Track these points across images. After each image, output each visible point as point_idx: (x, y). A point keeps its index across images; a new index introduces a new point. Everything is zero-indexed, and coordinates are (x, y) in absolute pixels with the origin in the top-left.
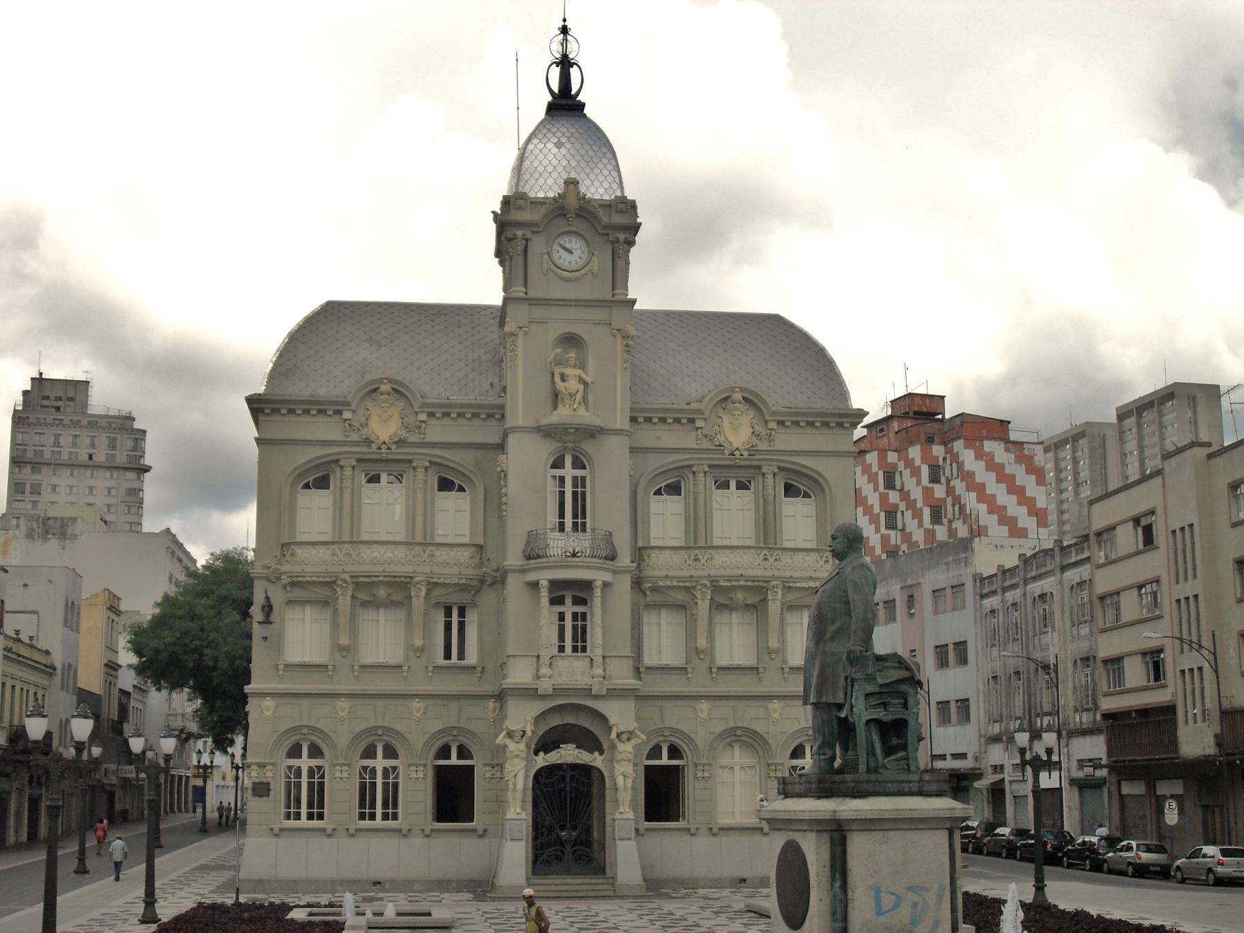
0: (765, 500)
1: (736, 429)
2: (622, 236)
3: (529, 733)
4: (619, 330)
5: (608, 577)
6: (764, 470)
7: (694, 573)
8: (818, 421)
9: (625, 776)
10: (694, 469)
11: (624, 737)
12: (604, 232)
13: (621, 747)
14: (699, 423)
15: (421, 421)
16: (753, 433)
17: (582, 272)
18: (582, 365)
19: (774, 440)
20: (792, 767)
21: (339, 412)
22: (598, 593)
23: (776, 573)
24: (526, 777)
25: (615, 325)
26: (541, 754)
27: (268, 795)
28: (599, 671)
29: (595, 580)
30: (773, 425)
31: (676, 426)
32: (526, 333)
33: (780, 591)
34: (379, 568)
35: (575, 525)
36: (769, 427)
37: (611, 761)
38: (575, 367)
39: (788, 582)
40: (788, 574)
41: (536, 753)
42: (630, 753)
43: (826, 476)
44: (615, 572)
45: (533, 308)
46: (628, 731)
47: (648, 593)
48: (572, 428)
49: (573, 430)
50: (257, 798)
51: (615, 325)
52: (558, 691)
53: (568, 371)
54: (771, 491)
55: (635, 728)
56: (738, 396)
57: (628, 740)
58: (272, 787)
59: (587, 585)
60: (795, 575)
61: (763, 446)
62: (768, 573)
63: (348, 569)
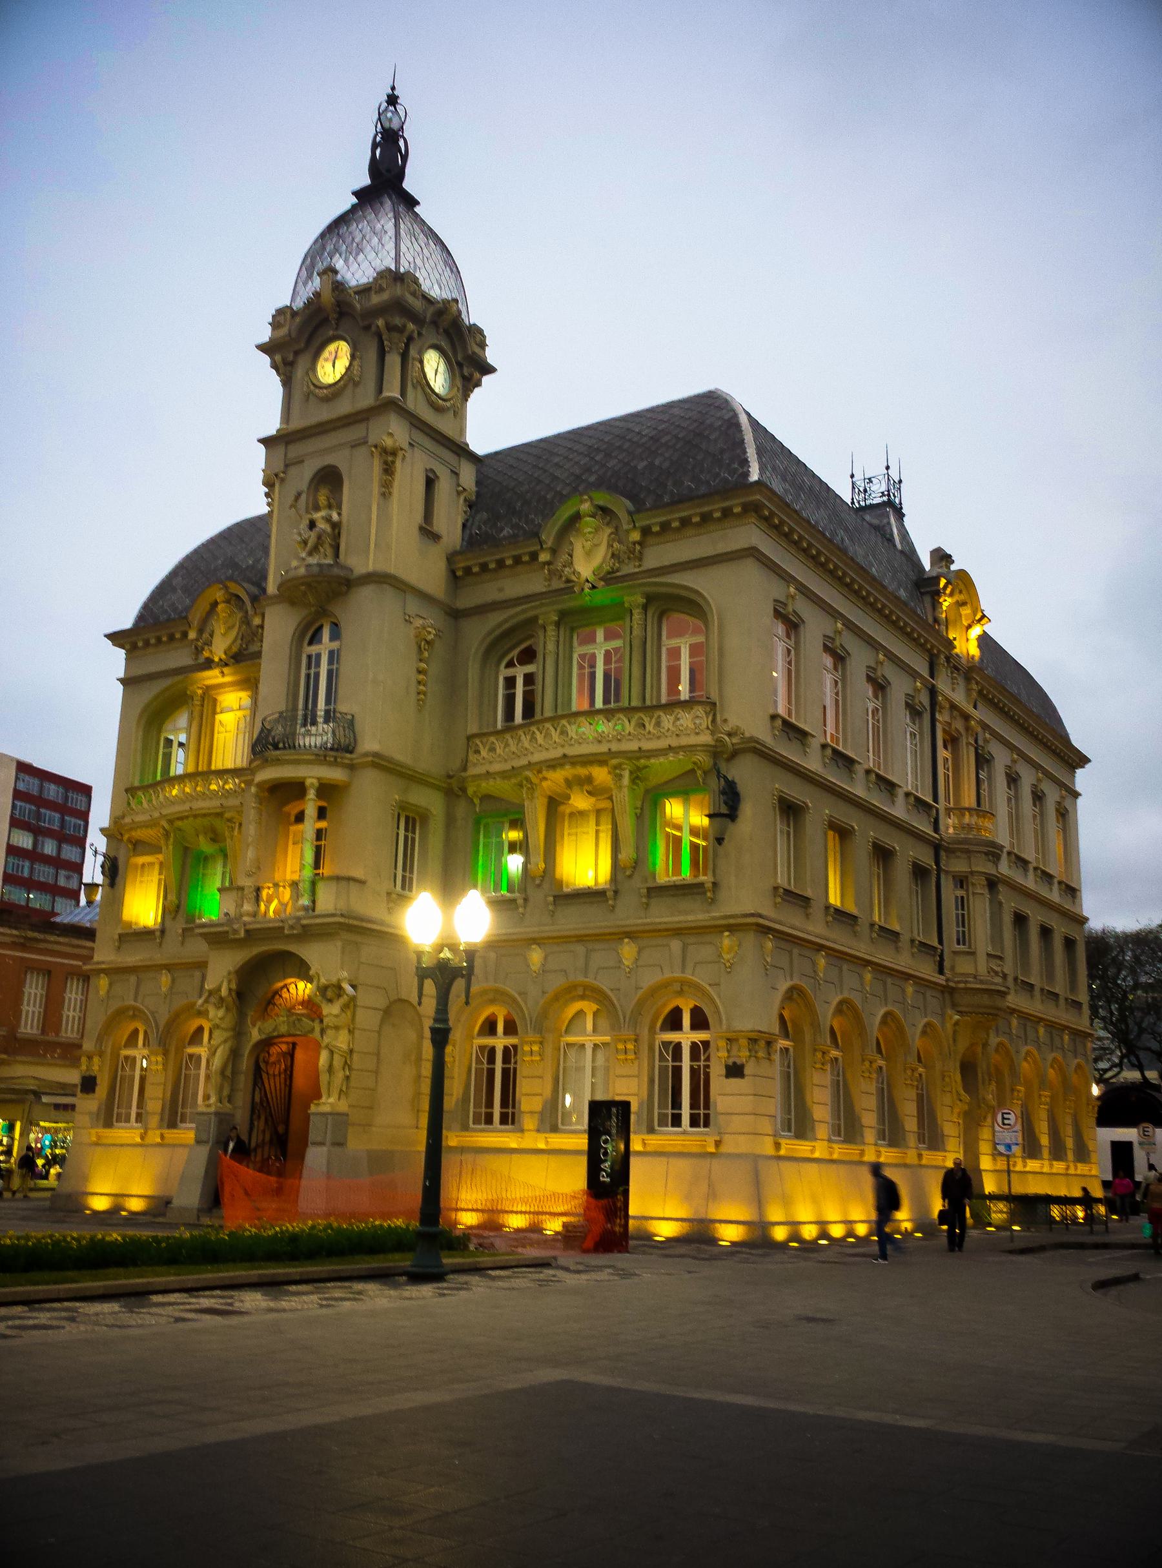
0: (631, 645)
1: (589, 554)
2: (380, 322)
3: (224, 992)
4: (376, 447)
5: (335, 775)
6: (626, 605)
7: (517, 763)
8: (695, 515)
9: (332, 1053)
10: (540, 622)
11: (329, 994)
12: (366, 323)
13: (325, 1011)
14: (544, 557)
15: (258, 626)
16: (613, 555)
17: (342, 383)
18: (335, 503)
19: (640, 559)
20: (663, 1043)
21: (185, 635)
22: (311, 794)
23: (615, 747)
24: (234, 1054)
25: (372, 440)
26: (259, 1024)
27: (93, 1091)
28: (305, 901)
29: (305, 778)
30: (636, 536)
31: (520, 568)
32: (282, 480)
33: (626, 774)
34: (186, 807)
35: (327, 712)
36: (631, 539)
37: (323, 1032)
38: (330, 507)
39: (638, 759)
40: (633, 746)
41: (254, 1025)
42: (336, 1016)
43: (705, 594)
44: (352, 767)
45: (291, 447)
46: (334, 985)
47: (476, 801)
48: (302, 584)
49: (303, 588)
50: (86, 1096)
51: (372, 440)
52: (252, 936)
53: (318, 516)
54: (637, 631)
55: (339, 980)
56: (586, 507)
57: (339, 996)
58: (98, 1081)
59: (296, 789)
60: (648, 745)
61: (629, 568)
62: (603, 748)
63: (164, 812)
